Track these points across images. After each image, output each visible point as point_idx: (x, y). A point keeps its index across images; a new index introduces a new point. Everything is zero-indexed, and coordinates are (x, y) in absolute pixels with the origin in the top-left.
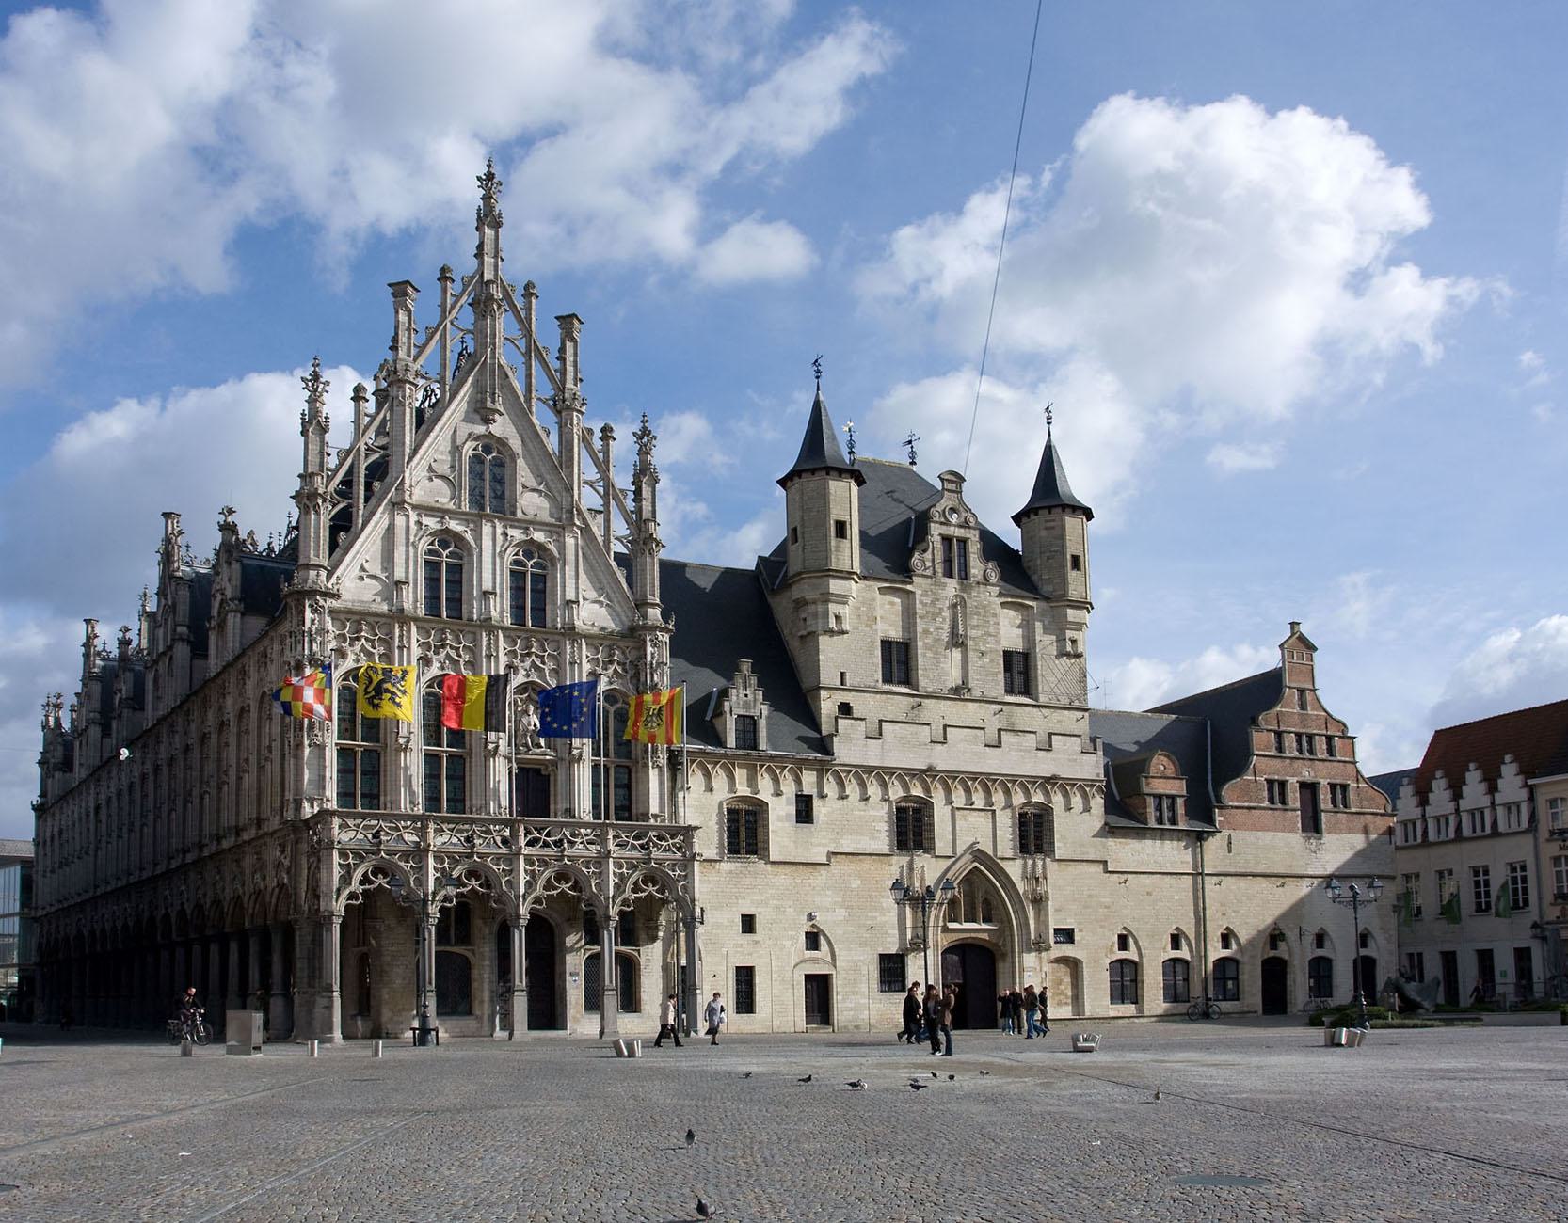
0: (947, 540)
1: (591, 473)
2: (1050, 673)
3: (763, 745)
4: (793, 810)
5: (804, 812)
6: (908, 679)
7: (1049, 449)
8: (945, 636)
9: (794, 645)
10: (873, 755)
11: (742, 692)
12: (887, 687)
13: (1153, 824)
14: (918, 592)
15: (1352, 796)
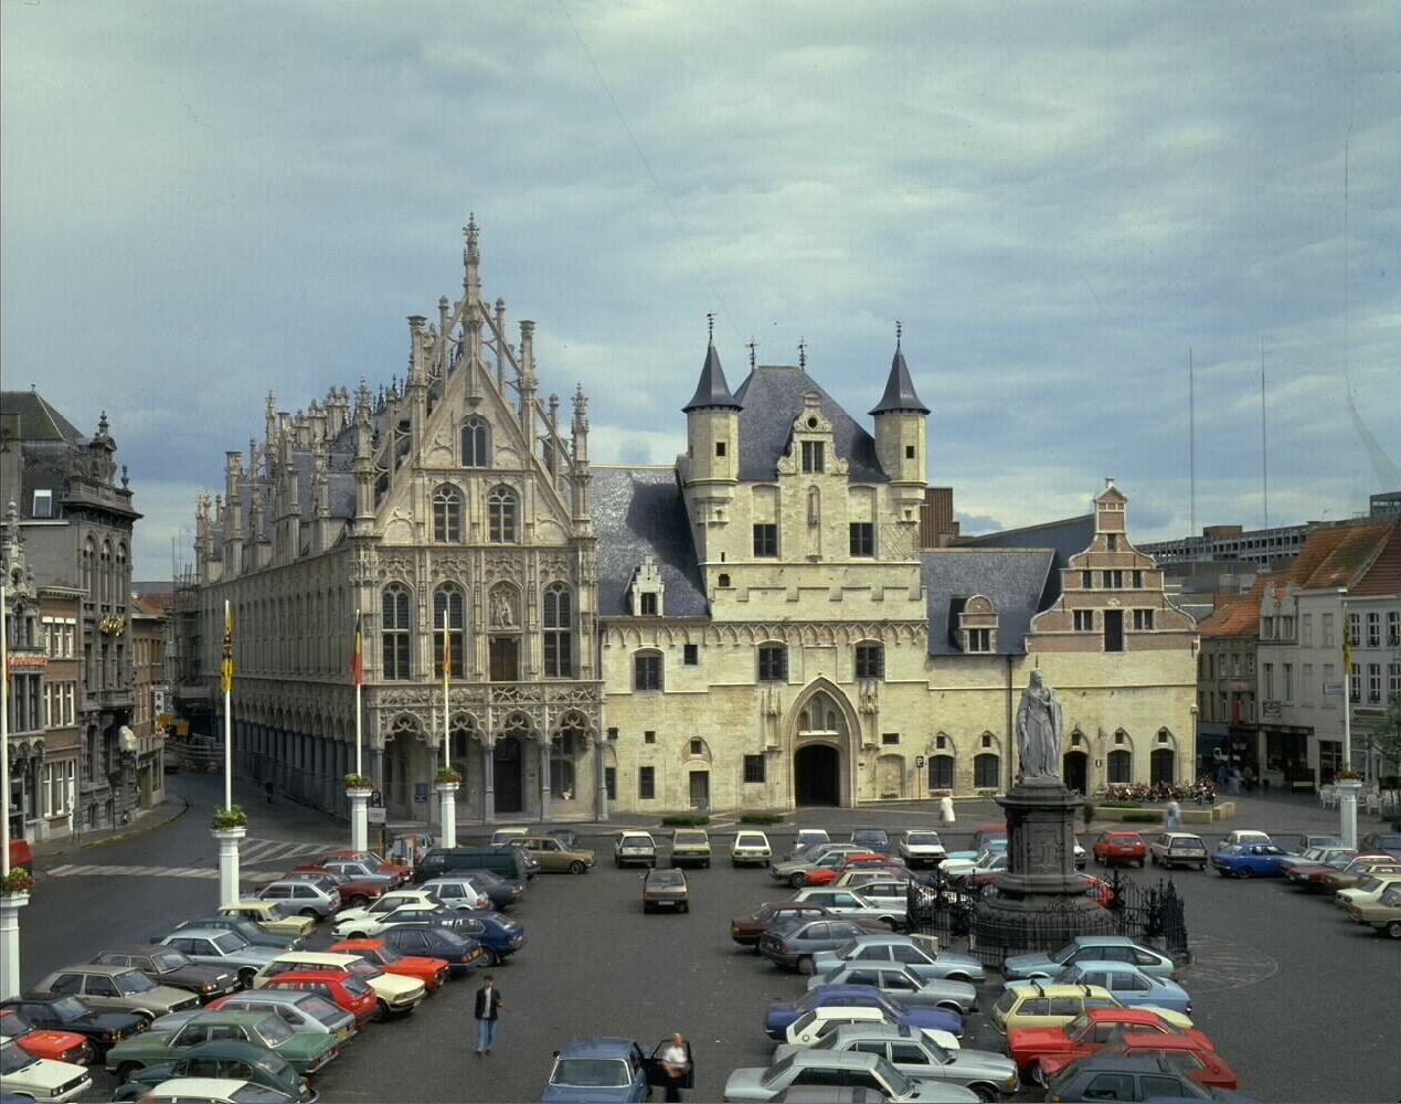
0: (806, 445)
3: (660, 612)
4: (682, 655)
5: (691, 655)
7: (898, 362)
8: (804, 519)
9: (693, 528)
13: (968, 651)
14: (783, 487)
15: (1155, 618)
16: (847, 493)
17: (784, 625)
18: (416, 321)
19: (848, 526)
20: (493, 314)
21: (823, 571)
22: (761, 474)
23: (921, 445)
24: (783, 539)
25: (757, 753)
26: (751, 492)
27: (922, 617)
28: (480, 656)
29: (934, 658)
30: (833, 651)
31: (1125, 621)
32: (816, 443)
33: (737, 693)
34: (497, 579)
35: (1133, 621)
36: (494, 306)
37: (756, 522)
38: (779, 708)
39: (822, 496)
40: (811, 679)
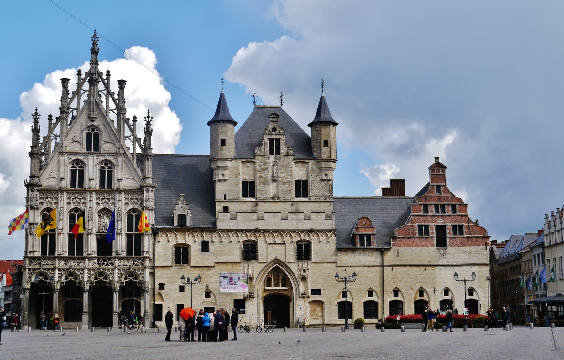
1: (128, 132)
2: (315, 189)
4: (200, 247)
5: (205, 247)
6: (253, 195)
8: (269, 177)
10: (232, 225)
11: (180, 205)
12: (244, 199)
14: (258, 162)
15: (464, 230)
16: (293, 165)
17: (257, 231)
18: (65, 82)
19: (294, 182)
20: (104, 77)
21: (279, 204)
22: (247, 155)
23: (332, 140)
24: (258, 188)
25: (241, 298)
26: (241, 164)
27: (332, 228)
28: (92, 245)
29: (339, 249)
30: (283, 246)
31: (447, 231)
32: (276, 140)
33: (230, 266)
34: (101, 207)
35: (452, 231)
36: (105, 73)
37: (243, 179)
38: (253, 274)
39: (279, 167)
40: (271, 259)
